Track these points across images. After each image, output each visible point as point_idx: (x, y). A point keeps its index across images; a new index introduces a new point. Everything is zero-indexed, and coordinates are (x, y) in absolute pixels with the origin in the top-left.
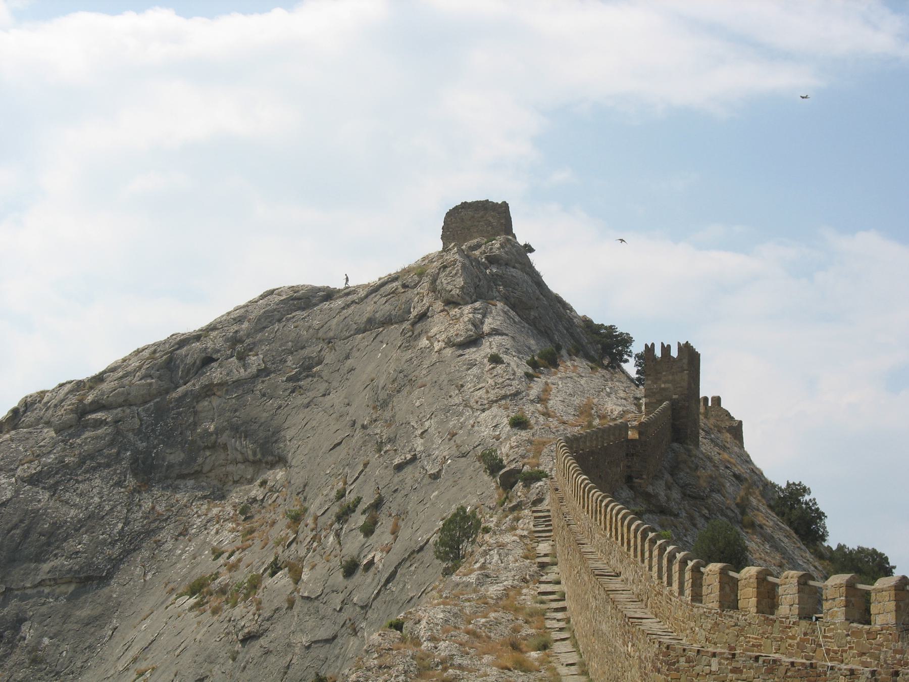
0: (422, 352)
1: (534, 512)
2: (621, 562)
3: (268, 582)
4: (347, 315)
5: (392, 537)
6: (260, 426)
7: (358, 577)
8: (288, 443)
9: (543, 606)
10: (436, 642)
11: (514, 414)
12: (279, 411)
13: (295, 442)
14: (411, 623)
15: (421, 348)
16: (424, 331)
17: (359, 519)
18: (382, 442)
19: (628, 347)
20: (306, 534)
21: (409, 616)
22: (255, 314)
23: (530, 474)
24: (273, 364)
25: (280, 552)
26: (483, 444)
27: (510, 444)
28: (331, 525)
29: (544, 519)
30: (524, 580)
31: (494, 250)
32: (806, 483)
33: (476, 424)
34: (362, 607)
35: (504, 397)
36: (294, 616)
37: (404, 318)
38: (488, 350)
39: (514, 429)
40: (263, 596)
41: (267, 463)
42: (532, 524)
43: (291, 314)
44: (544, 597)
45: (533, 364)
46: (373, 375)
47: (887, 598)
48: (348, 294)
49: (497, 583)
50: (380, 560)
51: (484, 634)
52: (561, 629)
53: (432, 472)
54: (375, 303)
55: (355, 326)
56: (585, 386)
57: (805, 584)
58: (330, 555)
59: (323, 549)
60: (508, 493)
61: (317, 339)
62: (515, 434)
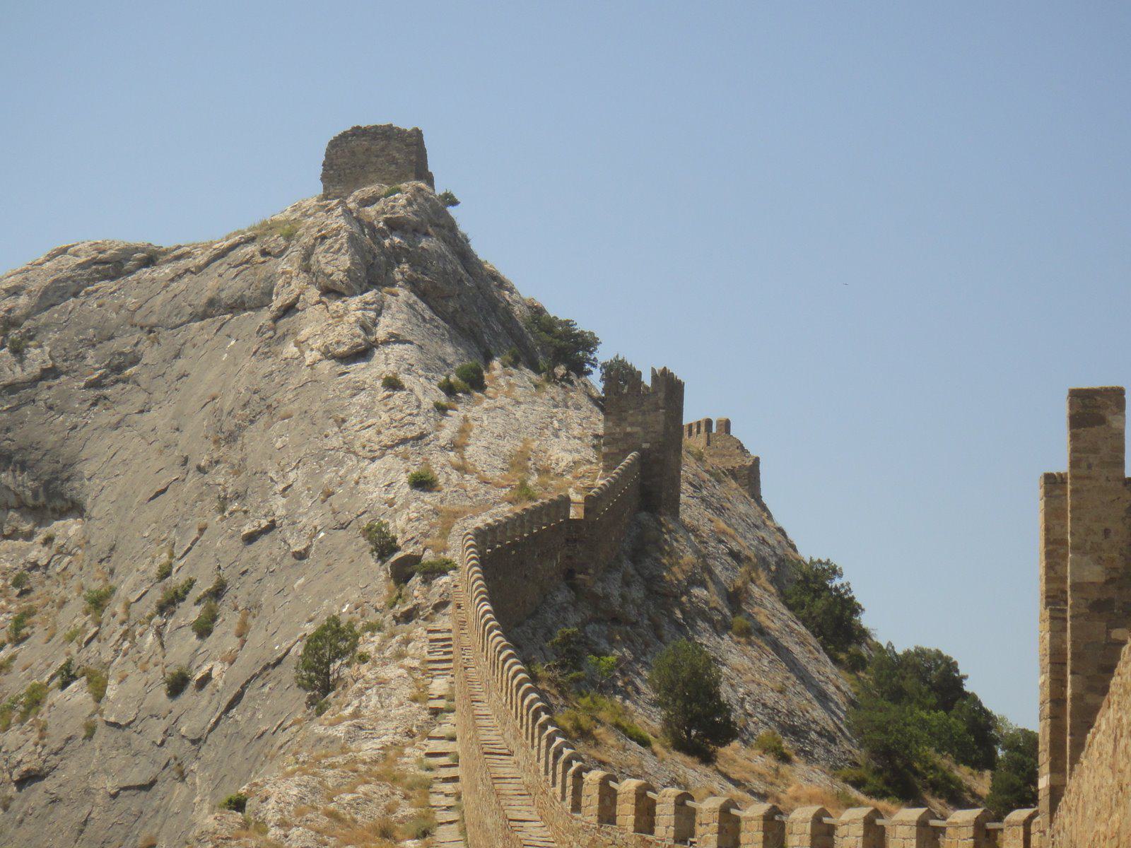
0: (287, 364)
1: (430, 632)
2: (515, 739)
3: (56, 696)
4: (177, 292)
5: (238, 640)
6: (45, 455)
7: (188, 695)
8: (87, 483)
9: (430, 775)
10: (286, 828)
11: (415, 467)
12: (73, 433)
13: (98, 481)
14: (257, 799)
15: (286, 359)
16: (290, 331)
17: (190, 612)
18: (225, 498)
19: (591, 353)
20: (114, 630)
21: (254, 788)
22: (39, 282)
23: (432, 565)
24: (65, 361)
25: (74, 652)
26: (370, 512)
27: (408, 514)
28: (151, 618)
29: (442, 644)
30: (410, 734)
31: (397, 209)
32: (837, 562)
33: (362, 480)
34: (194, 742)
35: (404, 441)
36: (94, 749)
37: (262, 302)
38: (383, 367)
39: (414, 491)
40: (49, 717)
41: (54, 510)
42: (426, 649)
43: (93, 285)
44: (432, 761)
45: (449, 389)
46: (214, 391)
47: (755, 829)
48: (178, 258)
49: (373, 738)
50: (220, 675)
51: (348, 817)
52: (449, 808)
53: (297, 549)
54: (220, 276)
55: (189, 310)
56: (521, 420)
57: (683, 804)
58: (148, 662)
59: (139, 652)
60: (401, 590)
61: (132, 325)
62: (417, 499)
